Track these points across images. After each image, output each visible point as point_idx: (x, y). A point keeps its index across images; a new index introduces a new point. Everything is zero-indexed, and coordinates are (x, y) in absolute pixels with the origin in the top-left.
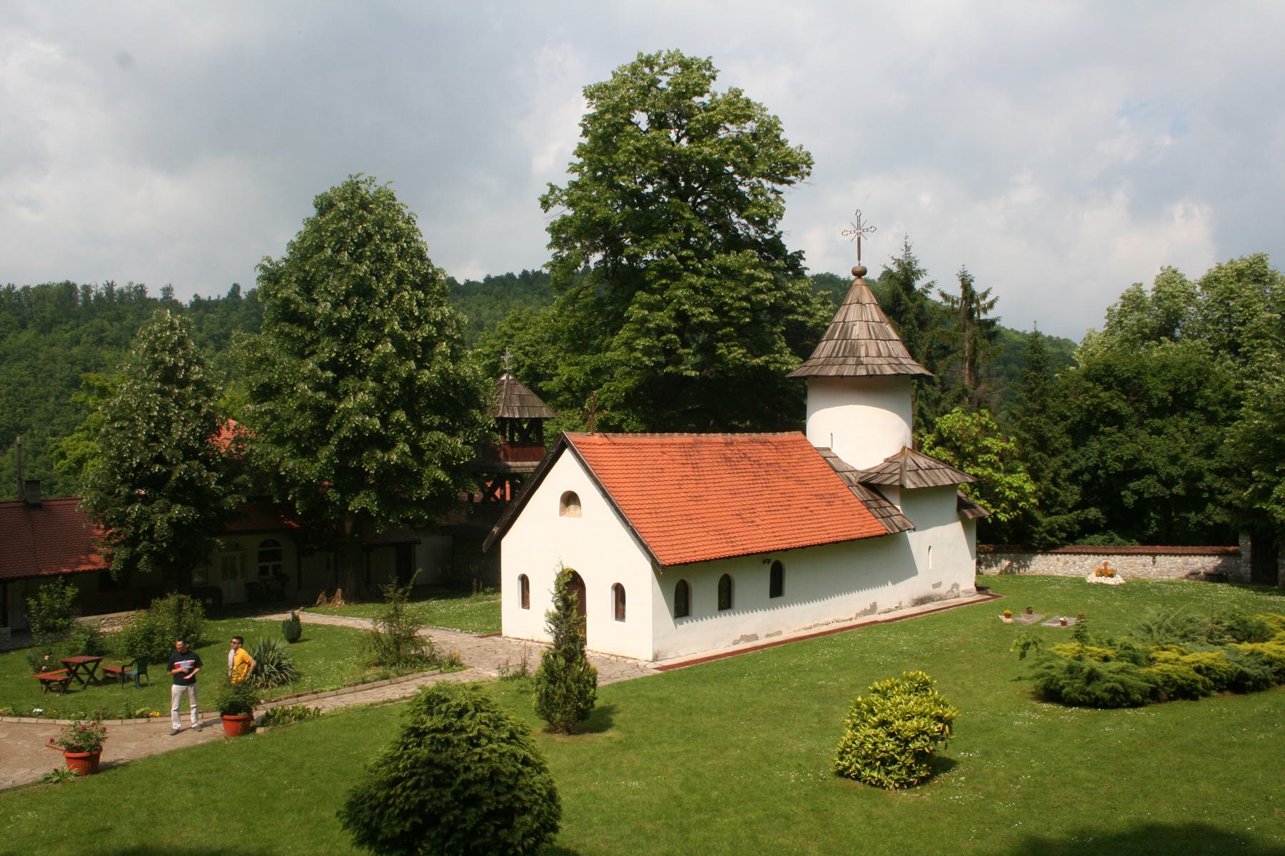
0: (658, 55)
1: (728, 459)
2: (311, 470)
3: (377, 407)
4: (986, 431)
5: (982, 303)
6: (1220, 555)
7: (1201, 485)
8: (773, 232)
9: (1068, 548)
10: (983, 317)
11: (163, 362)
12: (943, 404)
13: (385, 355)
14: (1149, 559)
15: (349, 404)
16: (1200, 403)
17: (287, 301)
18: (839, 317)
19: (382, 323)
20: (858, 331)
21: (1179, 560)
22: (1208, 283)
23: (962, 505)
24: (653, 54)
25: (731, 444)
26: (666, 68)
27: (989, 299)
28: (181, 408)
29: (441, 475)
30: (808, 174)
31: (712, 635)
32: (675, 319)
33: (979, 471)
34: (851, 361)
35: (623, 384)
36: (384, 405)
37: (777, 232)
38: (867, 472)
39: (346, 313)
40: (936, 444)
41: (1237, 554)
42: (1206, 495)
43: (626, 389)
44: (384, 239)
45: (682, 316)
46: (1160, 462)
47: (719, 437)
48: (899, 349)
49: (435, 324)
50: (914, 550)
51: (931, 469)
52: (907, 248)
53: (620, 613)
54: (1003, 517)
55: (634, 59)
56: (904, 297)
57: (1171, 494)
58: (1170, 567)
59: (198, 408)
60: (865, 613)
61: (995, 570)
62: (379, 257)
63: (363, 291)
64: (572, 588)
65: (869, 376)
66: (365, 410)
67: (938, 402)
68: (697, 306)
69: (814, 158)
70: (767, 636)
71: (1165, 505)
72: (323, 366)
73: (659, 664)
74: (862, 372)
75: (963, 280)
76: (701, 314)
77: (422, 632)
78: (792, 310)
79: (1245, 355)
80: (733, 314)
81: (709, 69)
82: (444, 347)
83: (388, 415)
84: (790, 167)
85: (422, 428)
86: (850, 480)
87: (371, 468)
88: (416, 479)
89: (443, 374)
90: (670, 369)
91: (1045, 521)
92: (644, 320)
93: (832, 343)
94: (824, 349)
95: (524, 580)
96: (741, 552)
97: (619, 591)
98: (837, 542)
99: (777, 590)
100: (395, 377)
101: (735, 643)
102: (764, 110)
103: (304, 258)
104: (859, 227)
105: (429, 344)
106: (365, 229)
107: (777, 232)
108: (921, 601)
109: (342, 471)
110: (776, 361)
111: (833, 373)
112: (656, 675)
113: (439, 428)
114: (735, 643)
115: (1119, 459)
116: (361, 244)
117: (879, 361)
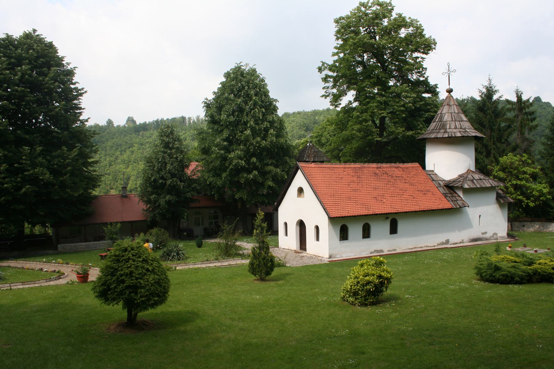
0: (368, 3)
1: (376, 174)
2: (219, 183)
3: (244, 156)
4: (525, 163)
8: (424, 77)
10: (527, 110)
12: (506, 152)
13: (248, 136)
15: (232, 155)
18: (439, 112)
20: (447, 118)
23: (499, 197)
24: (366, 2)
25: (380, 168)
28: (171, 158)
29: (270, 183)
30: (435, 49)
31: (357, 248)
33: (519, 182)
34: (442, 131)
35: (355, 145)
36: (248, 155)
37: (426, 76)
38: (449, 181)
39: (232, 119)
40: (499, 170)
43: (355, 148)
44: (249, 88)
47: (374, 165)
48: (467, 125)
49: (269, 122)
50: (471, 217)
51: (480, 179)
53: (318, 239)
54: (532, 204)
56: (488, 103)
59: (177, 158)
60: (443, 243)
61: (532, 229)
62: (248, 96)
63: (241, 110)
65: (449, 137)
67: (504, 151)
68: (381, 110)
69: (437, 41)
70: (388, 251)
72: (225, 140)
73: (331, 259)
75: (517, 93)
76: (383, 113)
77: (238, 243)
78: (428, 111)
80: (397, 113)
81: (390, 6)
82: (272, 131)
83: (250, 160)
84: (427, 46)
86: (440, 184)
87: (242, 181)
88: (262, 184)
89: (271, 142)
90: (370, 137)
92: (358, 117)
93: (435, 123)
94: (433, 125)
95: (286, 224)
96: (371, 213)
97: (317, 228)
98: (424, 211)
99: (394, 230)
100: (252, 144)
101: (371, 253)
102: (418, 22)
104: (449, 71)
105: (266, 130)
106: (242, 85)
107: (426, 76)
110: (419, 133)
111: (433, 137)
113: (271, 165)
114: (371, 253)
116: (239, 91)
117: (455, 131)
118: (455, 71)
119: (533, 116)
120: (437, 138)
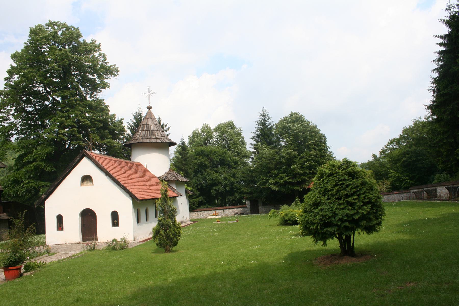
5: (165, 128)
6: (242, 207)
9: (198, 209)
14: (222, 211)
16: (227, 163)
21: (231, 210)
22: (218, 129)
26: (62, 28)
27: (167, 127)
34: (153, 137)
41: (246, 207)
42: (235, 190)
43: (47, 153)
52: (140, 108)
55: (48, 22)
58: (229, 212)
64: (88, 218)
65: (162, 142)
68: (83, 118)
74: (159, 141)
93: (144, 131)
111: (148, 141)
112: (140, 245)
115: (211, 179)
117: (163, 138)
120: (152, 142)
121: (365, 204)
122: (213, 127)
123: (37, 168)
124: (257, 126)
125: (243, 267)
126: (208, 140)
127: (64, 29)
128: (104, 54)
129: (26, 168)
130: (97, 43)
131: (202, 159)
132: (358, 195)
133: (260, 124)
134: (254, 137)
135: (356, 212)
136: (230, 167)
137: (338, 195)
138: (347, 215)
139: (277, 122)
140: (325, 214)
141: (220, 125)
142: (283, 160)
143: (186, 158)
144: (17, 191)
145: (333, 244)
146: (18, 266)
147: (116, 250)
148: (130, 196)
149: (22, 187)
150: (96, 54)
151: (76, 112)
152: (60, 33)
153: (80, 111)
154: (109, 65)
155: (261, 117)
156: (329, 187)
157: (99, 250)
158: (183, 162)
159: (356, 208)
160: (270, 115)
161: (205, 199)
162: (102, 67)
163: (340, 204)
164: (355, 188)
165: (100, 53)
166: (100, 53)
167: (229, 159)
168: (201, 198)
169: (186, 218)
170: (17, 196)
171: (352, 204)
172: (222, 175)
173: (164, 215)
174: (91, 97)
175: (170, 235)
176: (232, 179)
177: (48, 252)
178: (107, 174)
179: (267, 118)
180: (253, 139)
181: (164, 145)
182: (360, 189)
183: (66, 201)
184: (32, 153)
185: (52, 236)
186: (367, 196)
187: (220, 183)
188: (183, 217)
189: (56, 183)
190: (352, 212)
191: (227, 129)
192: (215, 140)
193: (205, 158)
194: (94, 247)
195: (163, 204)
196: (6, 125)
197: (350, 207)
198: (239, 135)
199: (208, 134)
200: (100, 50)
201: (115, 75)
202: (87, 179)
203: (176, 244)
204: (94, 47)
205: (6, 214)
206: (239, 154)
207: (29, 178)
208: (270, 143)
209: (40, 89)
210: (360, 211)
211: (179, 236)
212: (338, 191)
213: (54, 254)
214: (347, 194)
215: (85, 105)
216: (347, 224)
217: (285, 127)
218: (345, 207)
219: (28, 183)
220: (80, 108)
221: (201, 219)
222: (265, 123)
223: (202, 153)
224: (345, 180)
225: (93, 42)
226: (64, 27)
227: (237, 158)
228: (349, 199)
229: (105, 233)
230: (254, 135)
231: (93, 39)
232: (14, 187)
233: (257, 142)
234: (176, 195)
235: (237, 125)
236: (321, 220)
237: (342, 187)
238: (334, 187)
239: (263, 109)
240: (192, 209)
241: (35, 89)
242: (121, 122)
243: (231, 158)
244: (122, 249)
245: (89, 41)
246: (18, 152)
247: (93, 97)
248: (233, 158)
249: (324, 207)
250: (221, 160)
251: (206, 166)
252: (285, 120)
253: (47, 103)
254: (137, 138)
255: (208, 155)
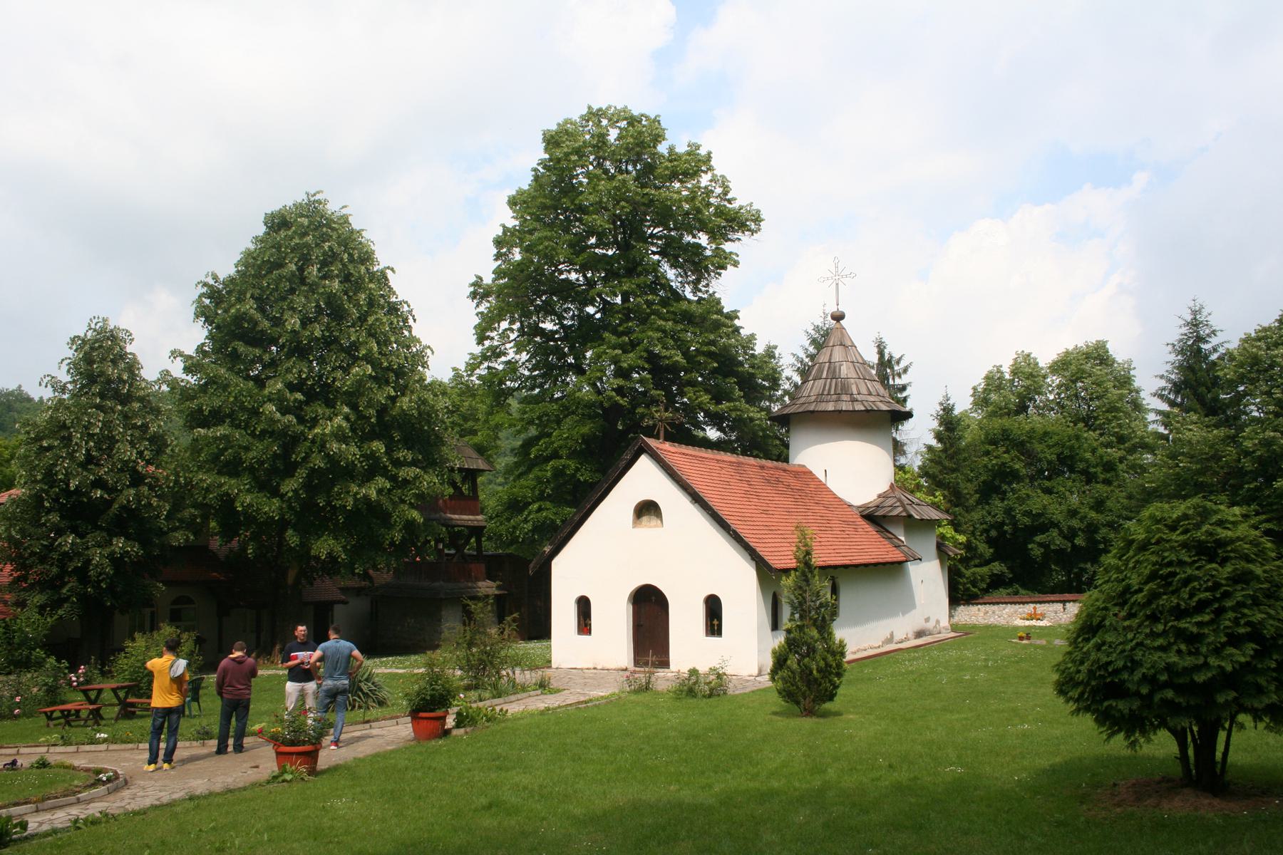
2: (271, 507)
5: (896, 368)
7: (1098, 537)
9: (987, 598)
10: (898, 381)
11: (102, 373)
14: (1060, 606)
16: (1081, 466)
17: (240, 318)
19: (355, 346)
22: (1061, 365)
27: (902, 365)
32: (648, 360)
34: (844, 397)
38: (865, 507)
42: (1102, 546)
43: (583, 436)
45: (652, 358)
46: (1058, 517)
55: (585, 111)
57: (1074, 546)
59: (145, 427)
62: (347, 278)
64: (649, 606)
65: (867, 411)
66: (340, 436)
68: (667, 349)
71: (1062, 557)
72: (291, 387)
74: (859, 407)
79: (1100, 427)
85: (398, 463)
91: (968, 573)
93: (820, 383)
103: (258, 276)
108: (919, 634)
109: (308, 507)
111: (831, 407)
115: (1028, 513)
117: (871, 399)
118: (852, 275)
119: (904, 394)
120: (840, 411)
121: (1235, 640)
122: (1045, 358)
123: (558, 473)
124: (1172, 357)
125: (916, 778)
126: (1030, 400)
127: (623, 124)
128: (723, 177)
129: (536, 472)
130: (703, 152)
131: (1005, 456)
132: (1219, 612)
133: (1182, 352)
134: (1164, 389)
135: (1201, 661)
136: (1090, 478)
137: (1154, 606)
138: (1169, 668)
139: (1234, 345)
140: (1105, 659)
141: (1067, 353)
142: (1247, 464)
143: (955, 453)
144: (514, 528)
145: (1161, 745)
146: (439, 713)
147: (695, 696)
148: (753, 559)
149: (526, 521)
150: (705, 180)
151: (650, 333)
152: (613, 135)
153: (659, 329)
154: (735, 205)
155: (1185, 330)
156: (1134, 581)
157: (658, 693)
158: (947, 463)
159: (1204, 650)
160: (1215, 322)
161: (1011, 569)
162: (720, 212)
163: (1153, 635)
164: (1207, 590)
165: (713, 175)
166: (713, 175)
167: (1088, 455)
168: (997, 567)
169: (938, 622)
170: (514, 541)
171: (1193, 640)
172: (1065, 502)
173: (801, 617)
174: (696, 290)
175: (811, 673)
176: (1093, 514)
177: (543, 685)
178: (696, 498)
179: (1204, 332)
180: (1161, 397)
181: (884, 420)
182: (1226, 595)
183: (598, 562)
184: (549, 435)
185: (565, 645)
186: (1244, 615)
187: (1055, 525)
188: (927, 620)
189: (577, 518)
190: (1189, 661)
191: (1087, 367)
192: (1051, 397)
193: (1014, 453)
194: (648, 683)
195: (800, 588)
196: (501, 367)
197: (1183, 647)
198: (1124, 381)
199: (1029, 382)
200: (710, 169)
201: (753, 232)
202: (647, 509)
203: (831, 697)
204: (694, 164)
205: (494, 584)
206: (1121, 439)
207: (541, 498)
208: (1212, 409)
209: (573, 276)
210: (1213, 661)
211: (839, 675)
212: (1154, 596)
213: (558, 691)
214: (1178, 605)
215: (674, 313)
216: (1169, 694)
217: (1255, 360)
218: (1170, 645)
219: (540, 510)
220: (661, 322)
221: (988, 627)
222: (1199, 349)
223: (1004, 439)
224: (1181, 563)
225: (693, 149)
226: (625, 119)
227: (1114, 453)
228: (1183, 624)
229: (689, 648)
230: (1163, 383)
231: (693, 141)
232: (508, 520)
233: (1172, 404)
234: (900, 557)
235: (1118, 353)
236: (1091, 673)
237: (1170, 584)
238: (1146, 583)
239: (1191, 304)
240: (959, 595)
241: (563, 277)
242: (770, 353)
243: (1094, 451)
244: (710, 696)
245: (681, 149)
246: (519, 432)
247: (700, 291)
248: (1101, 451)
249: (1110, 638)
250: (1062, 459)
251: (1015, 476)
252: (1259, 339)
253: (590, 310)
254: (802, 400)
255: (1022, 443)
